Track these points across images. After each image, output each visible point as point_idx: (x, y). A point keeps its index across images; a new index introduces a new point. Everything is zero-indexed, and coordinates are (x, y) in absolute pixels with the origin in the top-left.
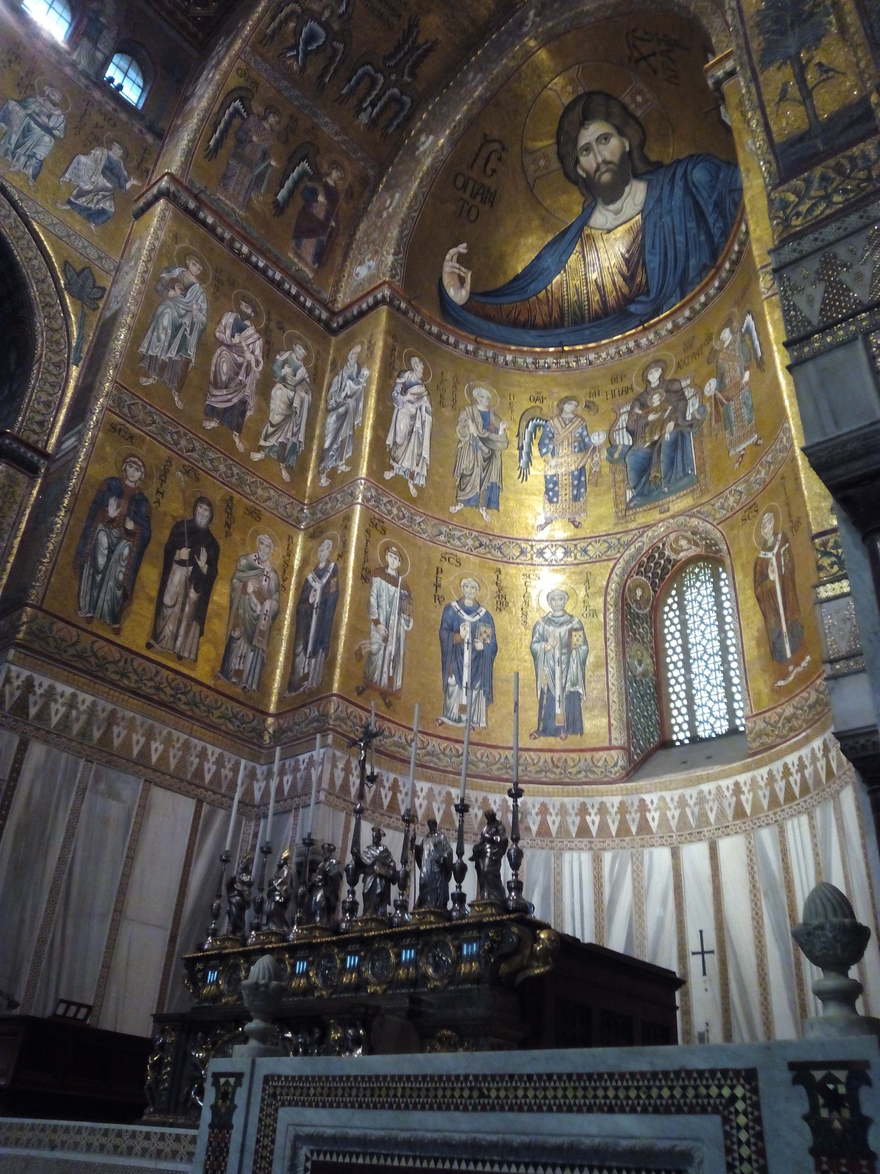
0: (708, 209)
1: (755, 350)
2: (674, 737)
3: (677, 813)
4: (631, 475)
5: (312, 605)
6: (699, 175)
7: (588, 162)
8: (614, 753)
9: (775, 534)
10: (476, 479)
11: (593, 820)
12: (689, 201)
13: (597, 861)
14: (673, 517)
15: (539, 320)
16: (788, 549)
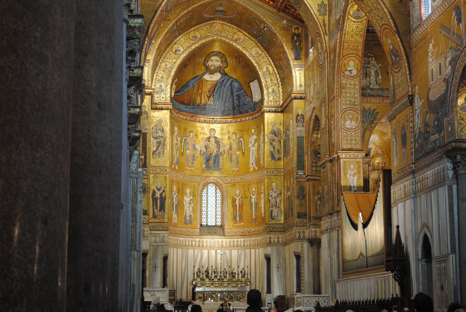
0: (235, 95)
1: (242, 149)
2: (202, 224)
3: (209, 244)
4: (205, 161)
5: (157, 197)
6: (236, 84)
7: (210, 63)
8: (197, 229)
9: (239, 195)
10: (175, 157)
11: (194, 243)
12: (230, 87)
13: (194, 251)
14: (214, 176)
15: (185, 103)
16: (242, 200)
